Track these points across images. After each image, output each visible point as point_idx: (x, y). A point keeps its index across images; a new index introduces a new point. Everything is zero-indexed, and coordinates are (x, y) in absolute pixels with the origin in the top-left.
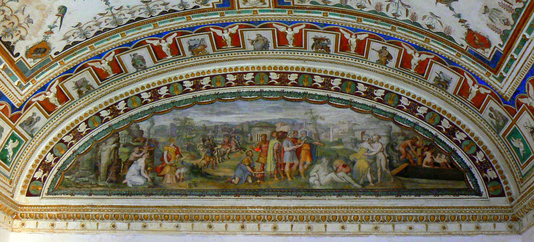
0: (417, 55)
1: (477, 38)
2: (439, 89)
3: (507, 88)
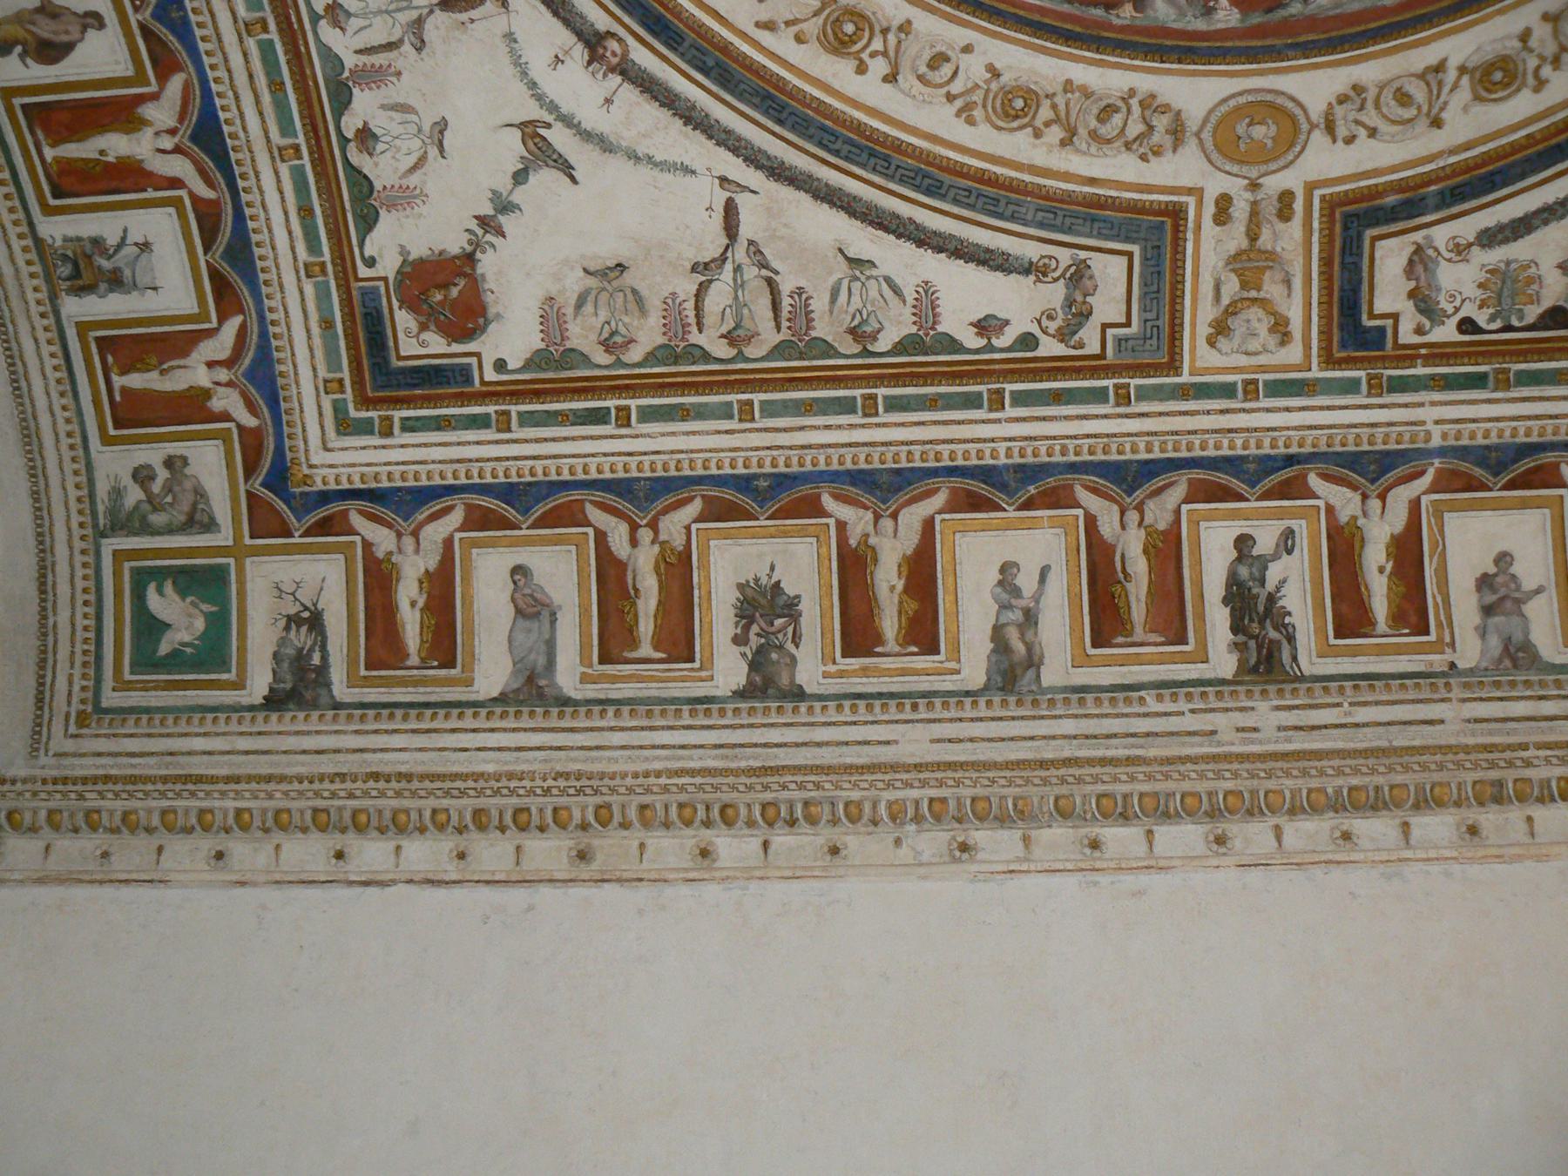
0: (167, 143)
1: (454, 292)
2: (37, 268)
3: (332, 458)
